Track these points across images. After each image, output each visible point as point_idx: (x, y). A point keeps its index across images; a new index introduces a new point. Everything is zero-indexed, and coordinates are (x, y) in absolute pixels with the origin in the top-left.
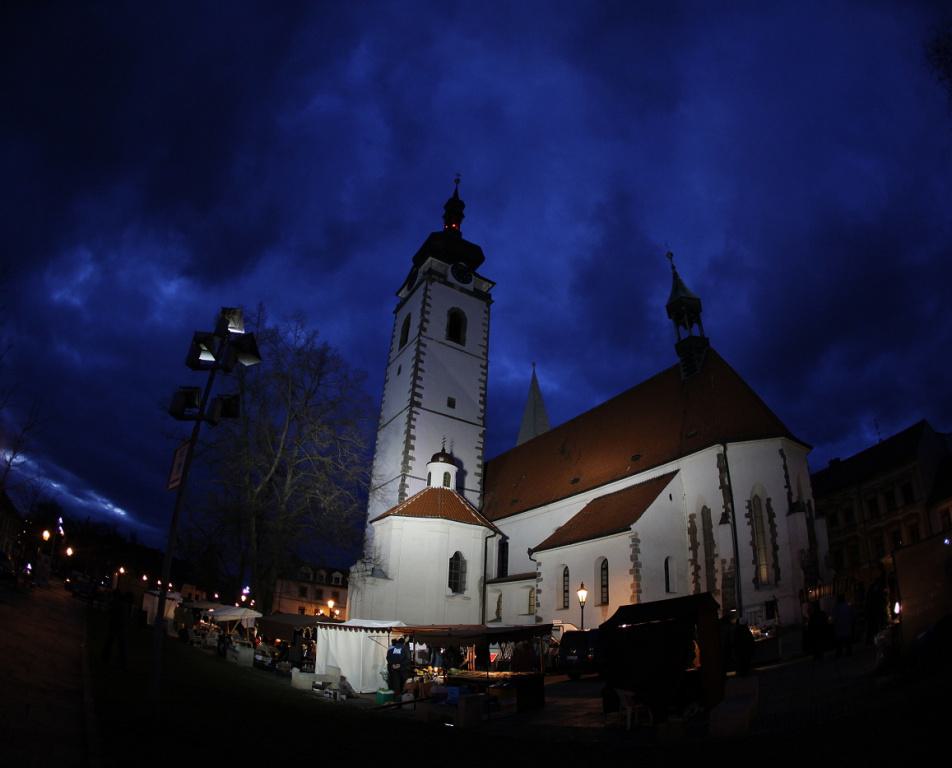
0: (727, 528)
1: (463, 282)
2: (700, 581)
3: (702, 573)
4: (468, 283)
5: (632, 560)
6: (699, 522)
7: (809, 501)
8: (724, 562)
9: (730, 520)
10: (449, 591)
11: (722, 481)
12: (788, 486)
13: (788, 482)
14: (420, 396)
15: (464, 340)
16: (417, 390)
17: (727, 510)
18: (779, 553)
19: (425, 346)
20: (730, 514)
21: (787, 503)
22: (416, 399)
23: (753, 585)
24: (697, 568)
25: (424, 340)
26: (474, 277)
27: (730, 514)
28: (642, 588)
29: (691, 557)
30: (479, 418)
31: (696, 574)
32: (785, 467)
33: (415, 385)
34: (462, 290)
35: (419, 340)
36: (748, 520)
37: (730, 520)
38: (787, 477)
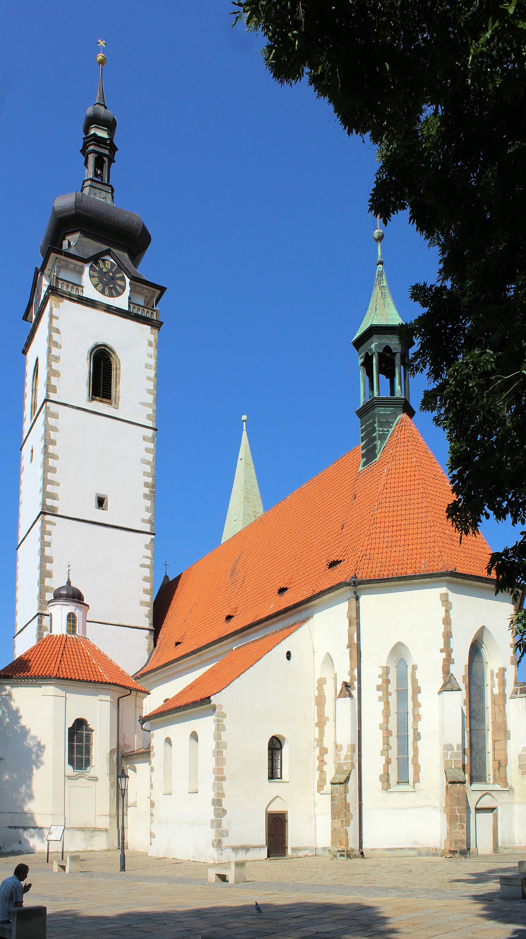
1: (111, 295)
4: (119, 294)
7: (503, 670)
9: (355, 693)
20: (356, 683)
21: (441, 674)
26: (128, 280)
29: (317, 736)
34: (109, 309)
36: (380, 693)
37: (355, 693)
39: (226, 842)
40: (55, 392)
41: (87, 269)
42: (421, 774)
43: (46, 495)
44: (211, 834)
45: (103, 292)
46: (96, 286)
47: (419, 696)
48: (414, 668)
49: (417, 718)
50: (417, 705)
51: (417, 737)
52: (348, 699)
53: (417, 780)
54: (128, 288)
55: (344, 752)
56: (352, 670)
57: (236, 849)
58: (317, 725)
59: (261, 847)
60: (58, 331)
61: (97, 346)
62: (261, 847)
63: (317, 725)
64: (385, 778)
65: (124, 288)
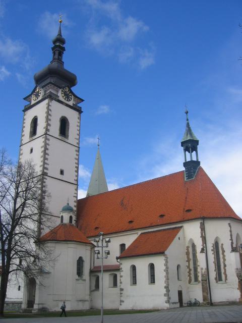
0: (204, 255)
2: (191, 276)
3: (192, 272)
4: (70, 101)
5: (165, 265)
6: (191, 250)
8: (202, 269)
9: (205, 251)
10: (77, 277)
11: (202, 234)
12: (231, 239)
13: (231, 237)
14: (47, 169)
15: (68, 136)
16: (46, 166)
17: (203, 247)
18: (226, 268)
19: (49, 140)
20: (205, 249)
22: (45, 171)
23: (215, 281)
24: (190, 270)
25: (48, 137)
27: (205, 249)
28: (169, 278)
30: (75, 180)
31: (189, 272)
32: (231, 231)
33: (44, 163)
35: (46, 137)
36: (213, 252)
37: (205, 251)
38: (231, 235)
39: (171, 301)
40: (49, 131)
41: (61, 90)
42: (228, 277)
43: (44, 168)
44: (166, 298)
45: (65, 99)
46: (63, 97)
47: (225, 253)
48: (222, 245)
49: (224, 260)
50: (224, 256)
51: (225, 266)
52: (204, 254)
53: (226, 279)
54: (72, 100)
55: (204, 271)
56: (203, 244)
57: (173, 303)
58: (187, 261)
59: (177, 303)
60: (50, 110)
61: (65, 117)
62: (177, 303)
63: (187, 261)
64: (216, 279)
65: (71, 99)
